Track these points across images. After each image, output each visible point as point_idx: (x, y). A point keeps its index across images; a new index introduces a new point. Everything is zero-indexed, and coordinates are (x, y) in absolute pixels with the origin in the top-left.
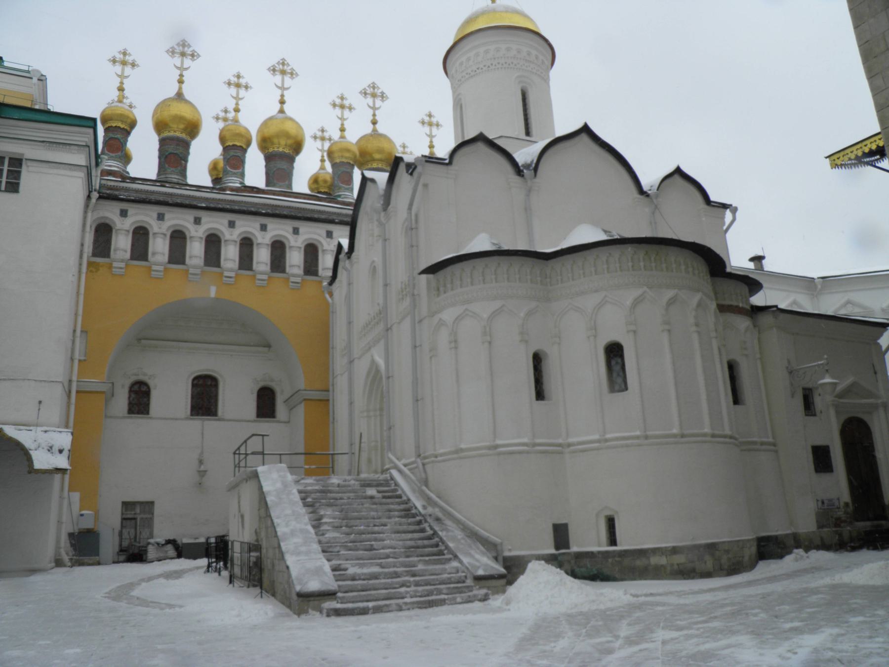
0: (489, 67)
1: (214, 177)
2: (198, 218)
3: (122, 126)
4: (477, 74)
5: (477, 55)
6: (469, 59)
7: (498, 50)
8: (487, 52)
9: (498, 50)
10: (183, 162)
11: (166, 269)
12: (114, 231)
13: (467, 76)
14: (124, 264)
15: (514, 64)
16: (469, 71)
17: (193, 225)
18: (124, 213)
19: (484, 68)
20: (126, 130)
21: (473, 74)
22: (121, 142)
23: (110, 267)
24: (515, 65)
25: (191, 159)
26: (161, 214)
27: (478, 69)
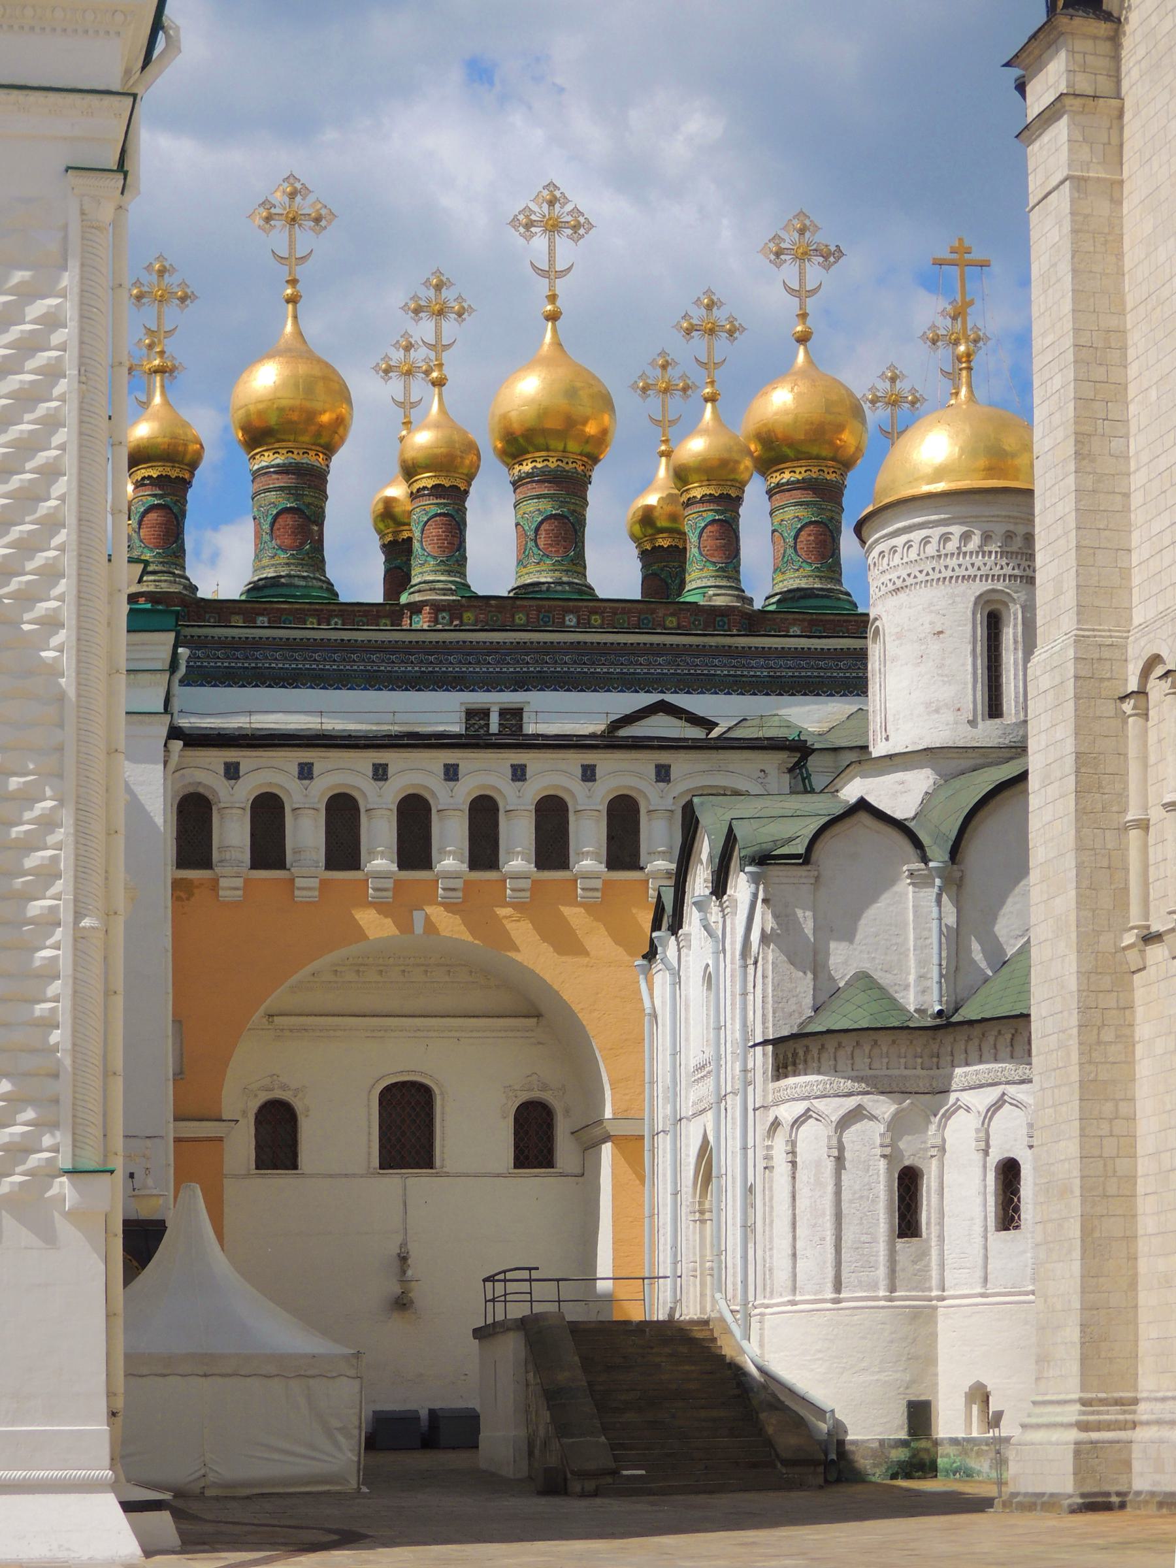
0: (928, 574)
1: (389, 538)
2: (380, 765)
3: (174, 474)
4: (906, 586)
5: (908, 545)
6: (893, 550)
7: (945, 538)
8: (926, 541)
9: (945, 538)
10: (316, 528)
11: (323, 883)
12: (214, 808)
13: (891, 587)
14: (241, 880)
15: (976, 568)
16: (893, 576)
17: (372, 781)
18: (232, 772)
19: (921, 577)
20: (183, 479)
21: (899, 583)
22: (173, 513)
23: (214, 885)
24: (979, 569)
25: (330, 508)
26: (306, 764)
27: (909, 575)
